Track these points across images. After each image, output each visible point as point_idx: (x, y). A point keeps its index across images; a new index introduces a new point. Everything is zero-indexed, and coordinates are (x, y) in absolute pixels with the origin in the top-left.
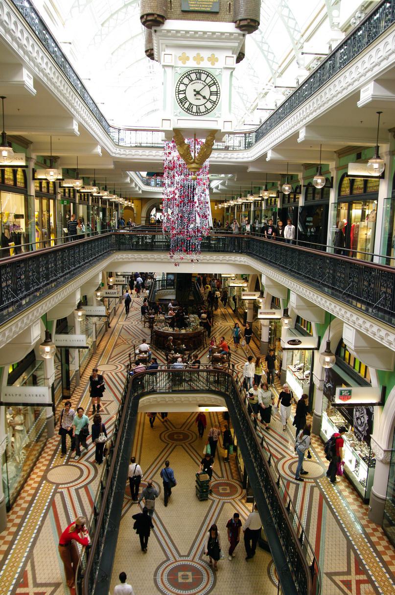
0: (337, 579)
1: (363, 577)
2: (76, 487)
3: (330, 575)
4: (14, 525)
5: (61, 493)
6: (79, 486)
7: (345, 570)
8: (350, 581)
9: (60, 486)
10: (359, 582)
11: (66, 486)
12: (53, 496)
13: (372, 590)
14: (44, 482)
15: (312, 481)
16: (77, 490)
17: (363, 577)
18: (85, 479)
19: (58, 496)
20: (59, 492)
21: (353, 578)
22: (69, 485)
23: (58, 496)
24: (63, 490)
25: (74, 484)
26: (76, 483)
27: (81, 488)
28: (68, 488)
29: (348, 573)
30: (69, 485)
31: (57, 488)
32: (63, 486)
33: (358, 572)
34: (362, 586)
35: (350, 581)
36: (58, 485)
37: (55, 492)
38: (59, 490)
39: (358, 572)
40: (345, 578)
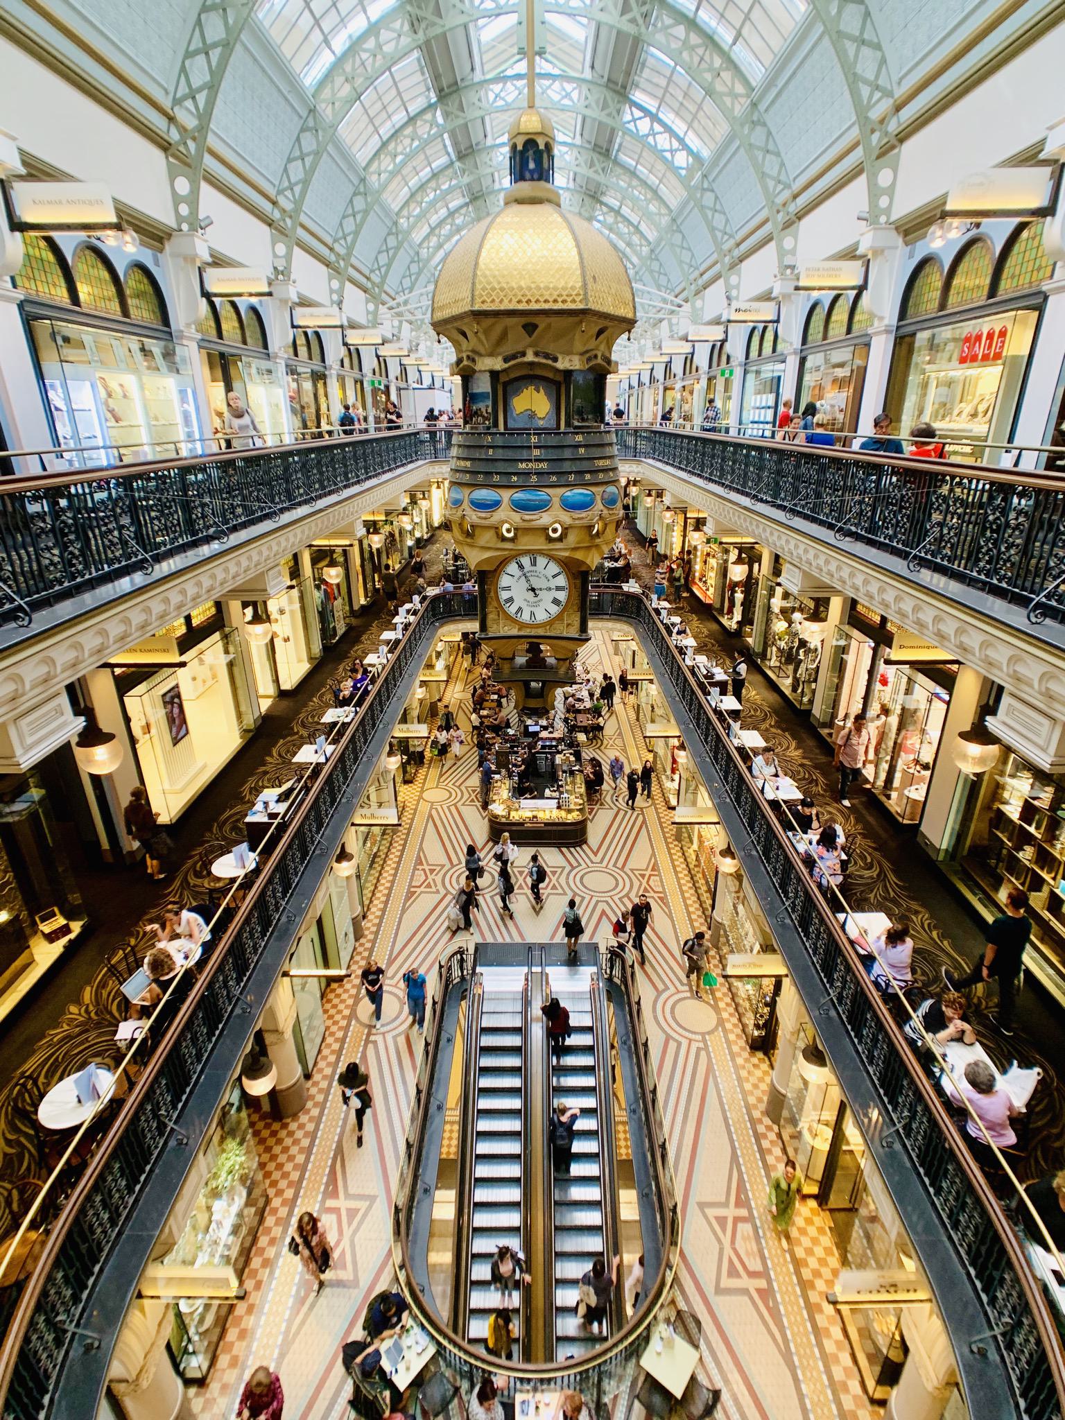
0: (711, 1212)
1: (743, 1212)
2: (394, 1033)
3: (702, 1206)
4: (316, 1105)
5: (375, 1042)
7: (723, 1199)
8: (725, 1218)
10: (737, 1220)
13: (751, 1233)
14: (353, 1022)
15: (700, 1038)
16: (395, 1038)
17: (743, 1212)
21: (731, 1212)
27: (399, 1035)
29: (725, 1205)
33: (738, 1204)
34: (740, 1226)
35: (725, 1218)
37: (367, 1041)
39: (738, 1204)
40: (721, 1212)
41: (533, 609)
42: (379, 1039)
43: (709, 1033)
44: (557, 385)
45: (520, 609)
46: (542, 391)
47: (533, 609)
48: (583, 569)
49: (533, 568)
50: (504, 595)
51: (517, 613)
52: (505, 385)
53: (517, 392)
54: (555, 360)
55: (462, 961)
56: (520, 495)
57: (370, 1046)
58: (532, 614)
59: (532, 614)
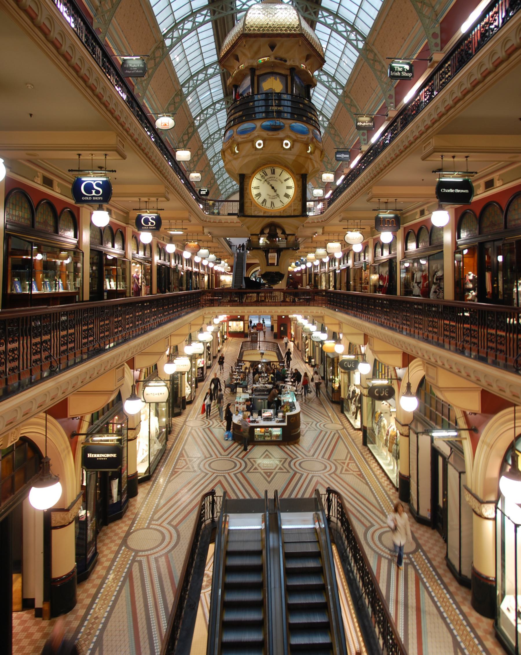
2: (156, 555)
5: (140, 562)
6: (159, 554)
9: (140, 554)
11: (146, 553)
12: (131, 565)
18: (166, 546)
19: (136, 565)
20: (137, 561)
22: (146, 553)
23: (136, 565)
24: (142, 558)
25: (152, 552)
26: (157, 550)
28: (147, 556)
30: (149, 552)
31: (135, 557)
32: (143, 553)
36: (137, 552)
37: (134, 561)
38: (138, 558)
41: (273, 200)
42: (144, 560)
43: (412, 553)
44: (286, 76)
45: (265, 201)
46: (278, 80)
47: (273, 200)
48: (303, 172)
49: (273, 175)
50: (254, 192)
51: (263, 203)
52: (259, 76)
53: (264, 80)
54: (286, 61)
55: (213, 503)
56: (267, 123)
57: (136, 564)
58: (272, 203)
59: (272, 203)
